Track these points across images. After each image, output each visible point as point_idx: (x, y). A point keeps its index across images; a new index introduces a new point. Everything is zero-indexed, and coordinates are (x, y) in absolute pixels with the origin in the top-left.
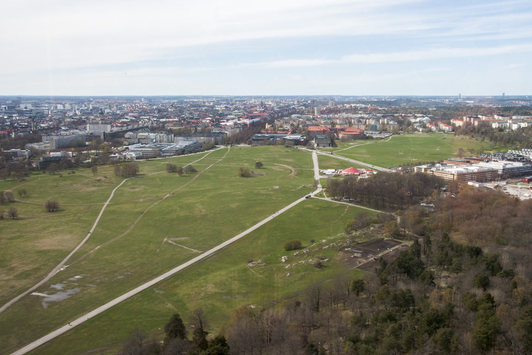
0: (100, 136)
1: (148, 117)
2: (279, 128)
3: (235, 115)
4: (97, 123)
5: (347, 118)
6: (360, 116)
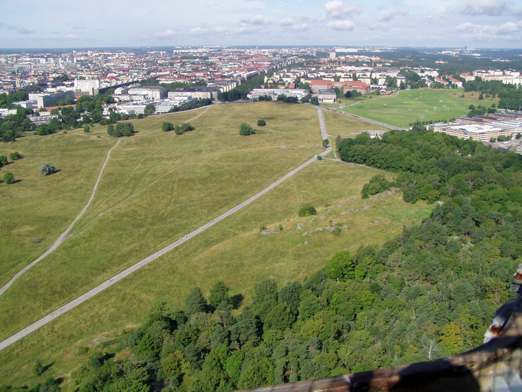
0: (89, 92)
1: (137, 71)
2: (280, 82)
3: (231, 68)
4: (84, 78)
5: (350, 71)
6: (364, 68)
